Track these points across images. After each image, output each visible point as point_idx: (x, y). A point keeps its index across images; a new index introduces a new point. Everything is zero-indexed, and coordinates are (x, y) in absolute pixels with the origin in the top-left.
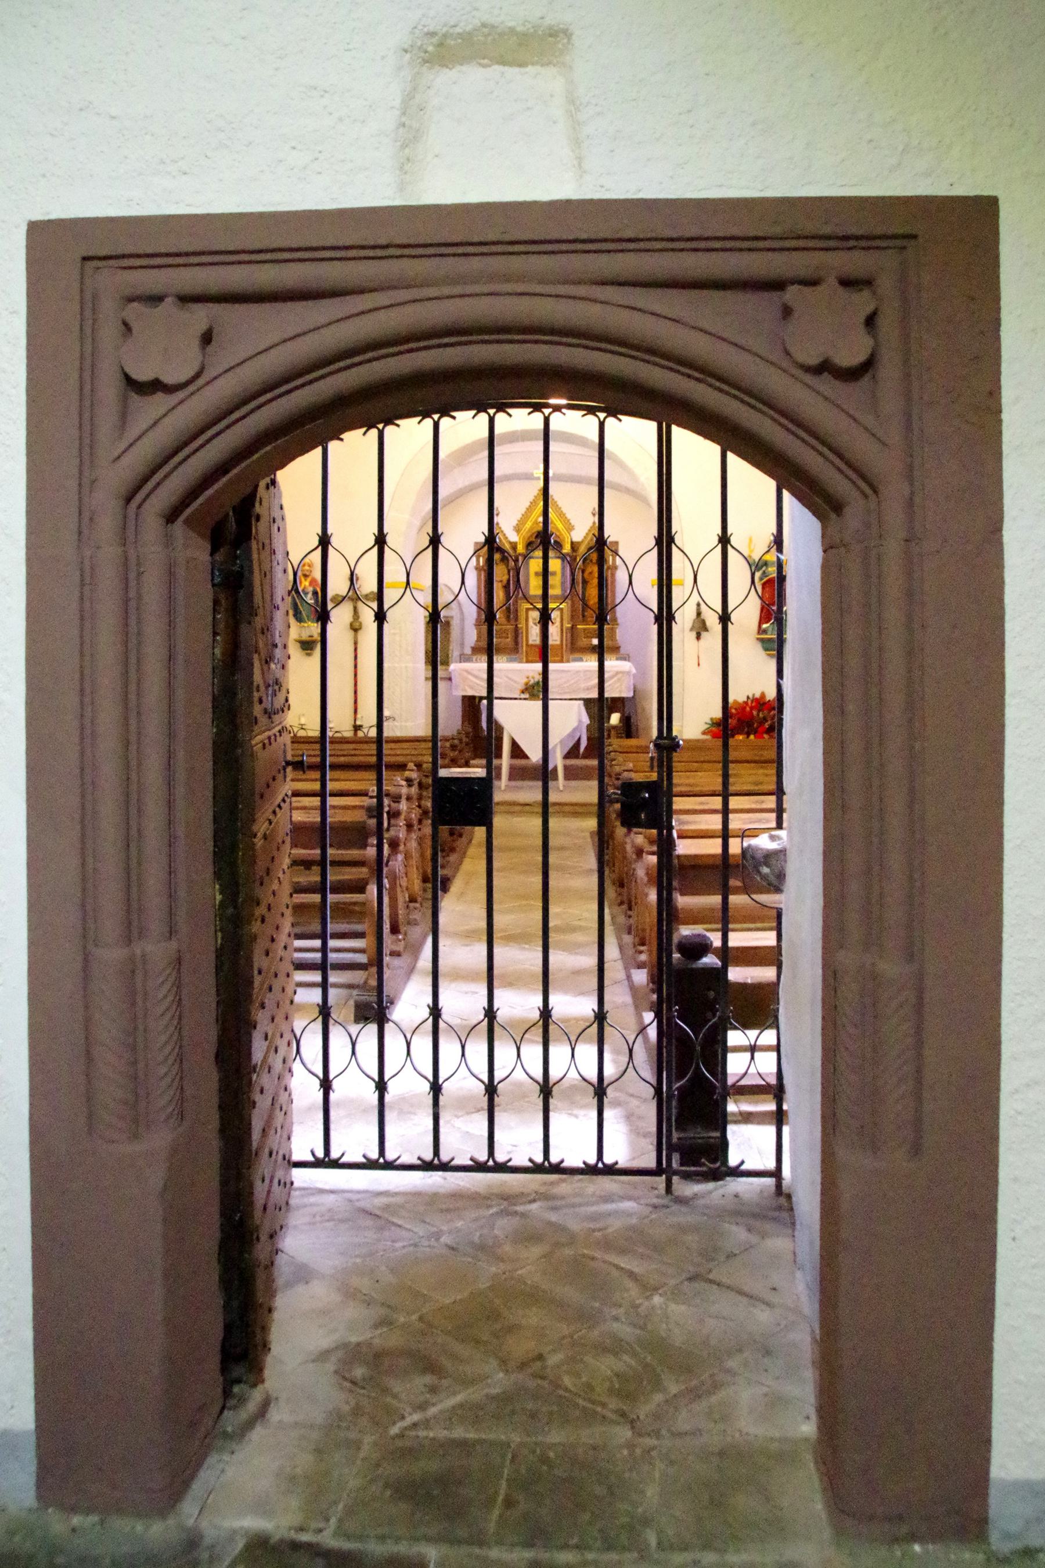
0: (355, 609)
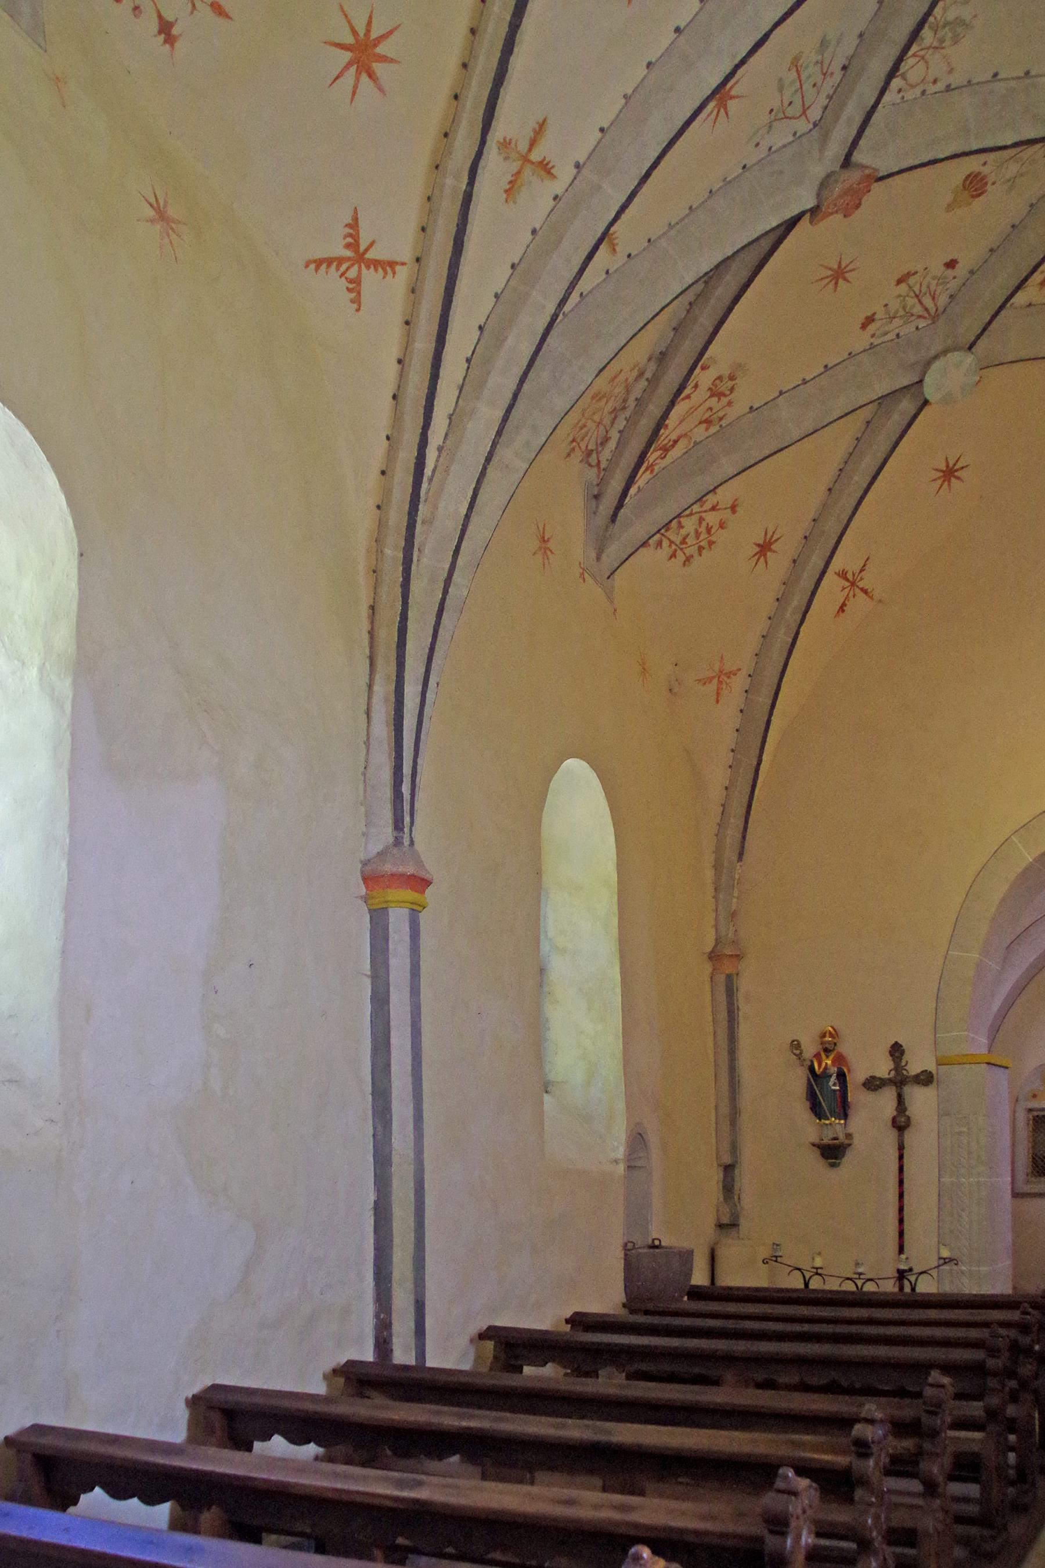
0: (900, 1099)
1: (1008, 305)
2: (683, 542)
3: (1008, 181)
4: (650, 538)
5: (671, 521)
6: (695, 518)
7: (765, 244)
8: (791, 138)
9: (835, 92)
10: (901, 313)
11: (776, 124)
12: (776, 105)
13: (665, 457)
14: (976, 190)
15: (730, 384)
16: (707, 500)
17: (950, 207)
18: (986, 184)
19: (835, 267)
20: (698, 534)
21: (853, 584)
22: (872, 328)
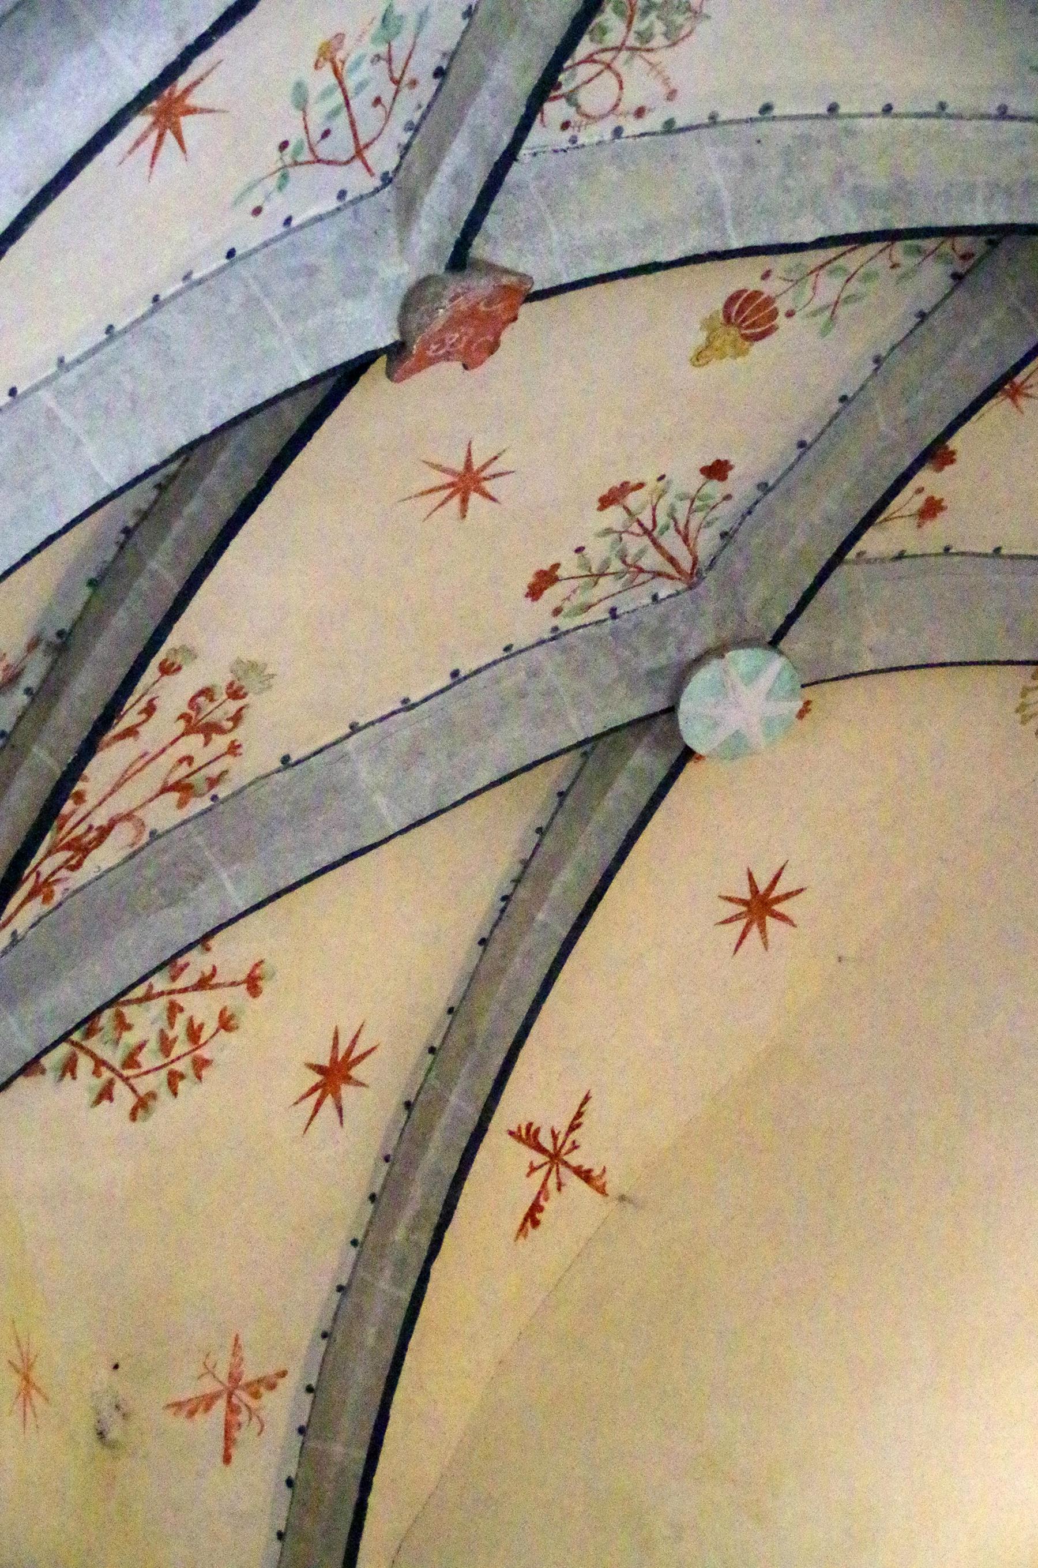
1: (851, 555)
2: (131, 1061)
3: (821, 310)
4: (46, 1051)
5: (99, 1011)
6: (158, 1007)
7: (293, 416)
8: (333, 203)
9: (424, 117)
10: (616, 565)
11: (294, 172)
12: (295, 135)
13: (79, 865)
14: (753, 325)
15: (233, 706)
16: (187, 965)
17: (699, 358)
18: (774, 314)
19: (460, 468)
20: (166, 1045)
21: (555, 1158)
22: (553, 595)
